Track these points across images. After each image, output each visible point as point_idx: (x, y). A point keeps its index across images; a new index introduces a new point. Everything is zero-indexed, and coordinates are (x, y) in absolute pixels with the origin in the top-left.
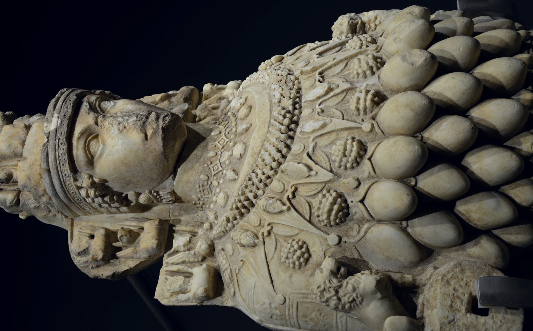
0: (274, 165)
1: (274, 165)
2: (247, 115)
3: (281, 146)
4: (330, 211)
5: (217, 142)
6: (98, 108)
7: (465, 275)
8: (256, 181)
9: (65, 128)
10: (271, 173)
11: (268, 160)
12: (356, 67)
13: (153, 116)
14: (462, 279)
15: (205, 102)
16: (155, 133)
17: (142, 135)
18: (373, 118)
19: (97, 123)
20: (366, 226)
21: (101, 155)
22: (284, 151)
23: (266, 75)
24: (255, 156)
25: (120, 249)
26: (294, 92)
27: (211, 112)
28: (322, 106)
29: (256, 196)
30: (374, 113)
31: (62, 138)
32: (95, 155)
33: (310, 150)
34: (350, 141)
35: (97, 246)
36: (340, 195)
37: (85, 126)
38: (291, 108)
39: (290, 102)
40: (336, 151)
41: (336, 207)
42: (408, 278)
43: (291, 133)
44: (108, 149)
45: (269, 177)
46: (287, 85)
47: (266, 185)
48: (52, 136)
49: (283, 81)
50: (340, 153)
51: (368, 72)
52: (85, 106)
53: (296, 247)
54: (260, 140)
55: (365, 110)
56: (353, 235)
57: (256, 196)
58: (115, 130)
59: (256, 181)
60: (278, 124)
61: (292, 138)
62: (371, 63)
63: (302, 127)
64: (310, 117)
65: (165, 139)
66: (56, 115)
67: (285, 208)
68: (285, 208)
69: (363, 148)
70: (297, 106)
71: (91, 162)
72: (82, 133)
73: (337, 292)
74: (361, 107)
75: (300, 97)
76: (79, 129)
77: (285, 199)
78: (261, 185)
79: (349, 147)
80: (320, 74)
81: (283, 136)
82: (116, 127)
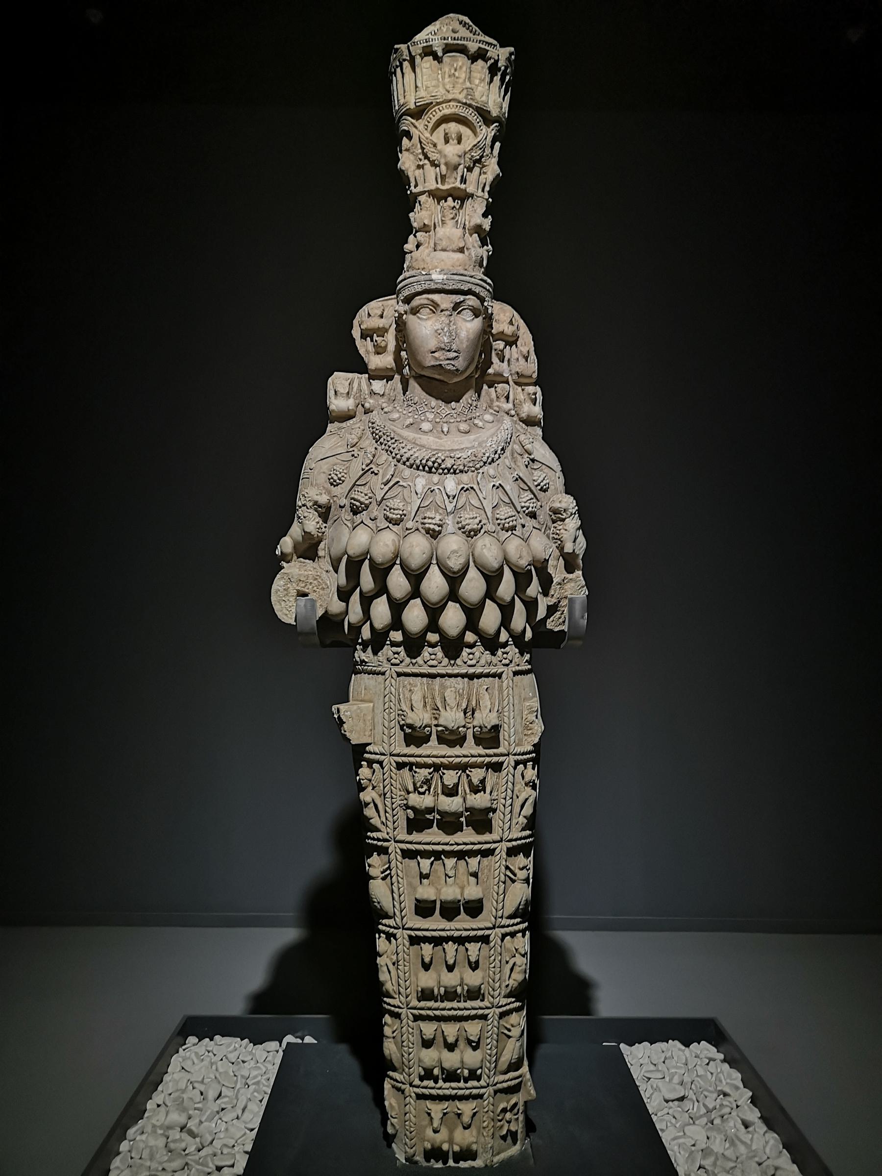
0: (398, 457)
1: (398, 457)
2: (459, 431)
3: (411, 461)
4: (355, 500)
8: (389, 443)
9: (433, 286)
10: (394, 455)
11: (402, 451)
12: (467, 516)
13: (453, 355)
15: (520, 389)
16: (436, 359)
17: (434, 350)
18: (418, 529)
19: (442, 311)
21: (419, 318)
22: (408, 463)
25: (372, 340)
26: (461, 467)
28: (437, 491)
29: (381, 444)
30: (420, 529)
31: (426, 286)
33: (401, 483)
34: (401, 512)
35: (375, 323)
36: (367, 506)
37: (439, 303)
38: (443, 466)
39: (449, 466)
40: (396, 503)
41: (358, 504)
42: (321, 553)
43: (421, 468)
44: (423, 323)
45: (391, 453)
47: (387, 451)
48: (427, 277)
49: (474, 458)
50: (392, 506)
51: (460, 525)
52: (459, 298)
53: (340, 476)
55: (423, 523)
56: (346, 515)
57: (381, 444)
58: (438, 326)
59: (389, 443)
61: (418, 468)
62: (468, 528)
64: (429, 482)
66: (445, 277)
67: (364, 467)
68: (364, 467)
69: (397, 523)
70: (446, 471)
71: (415, 311)
72: (432, 301)
73: (304, 505)
74: (426, 521)
75: (455, 473)
76: (436, 297)
77: (371, 466)
79: (396, 512)
80: (472, 488)
81: (418, 462)
82: (439, 327)
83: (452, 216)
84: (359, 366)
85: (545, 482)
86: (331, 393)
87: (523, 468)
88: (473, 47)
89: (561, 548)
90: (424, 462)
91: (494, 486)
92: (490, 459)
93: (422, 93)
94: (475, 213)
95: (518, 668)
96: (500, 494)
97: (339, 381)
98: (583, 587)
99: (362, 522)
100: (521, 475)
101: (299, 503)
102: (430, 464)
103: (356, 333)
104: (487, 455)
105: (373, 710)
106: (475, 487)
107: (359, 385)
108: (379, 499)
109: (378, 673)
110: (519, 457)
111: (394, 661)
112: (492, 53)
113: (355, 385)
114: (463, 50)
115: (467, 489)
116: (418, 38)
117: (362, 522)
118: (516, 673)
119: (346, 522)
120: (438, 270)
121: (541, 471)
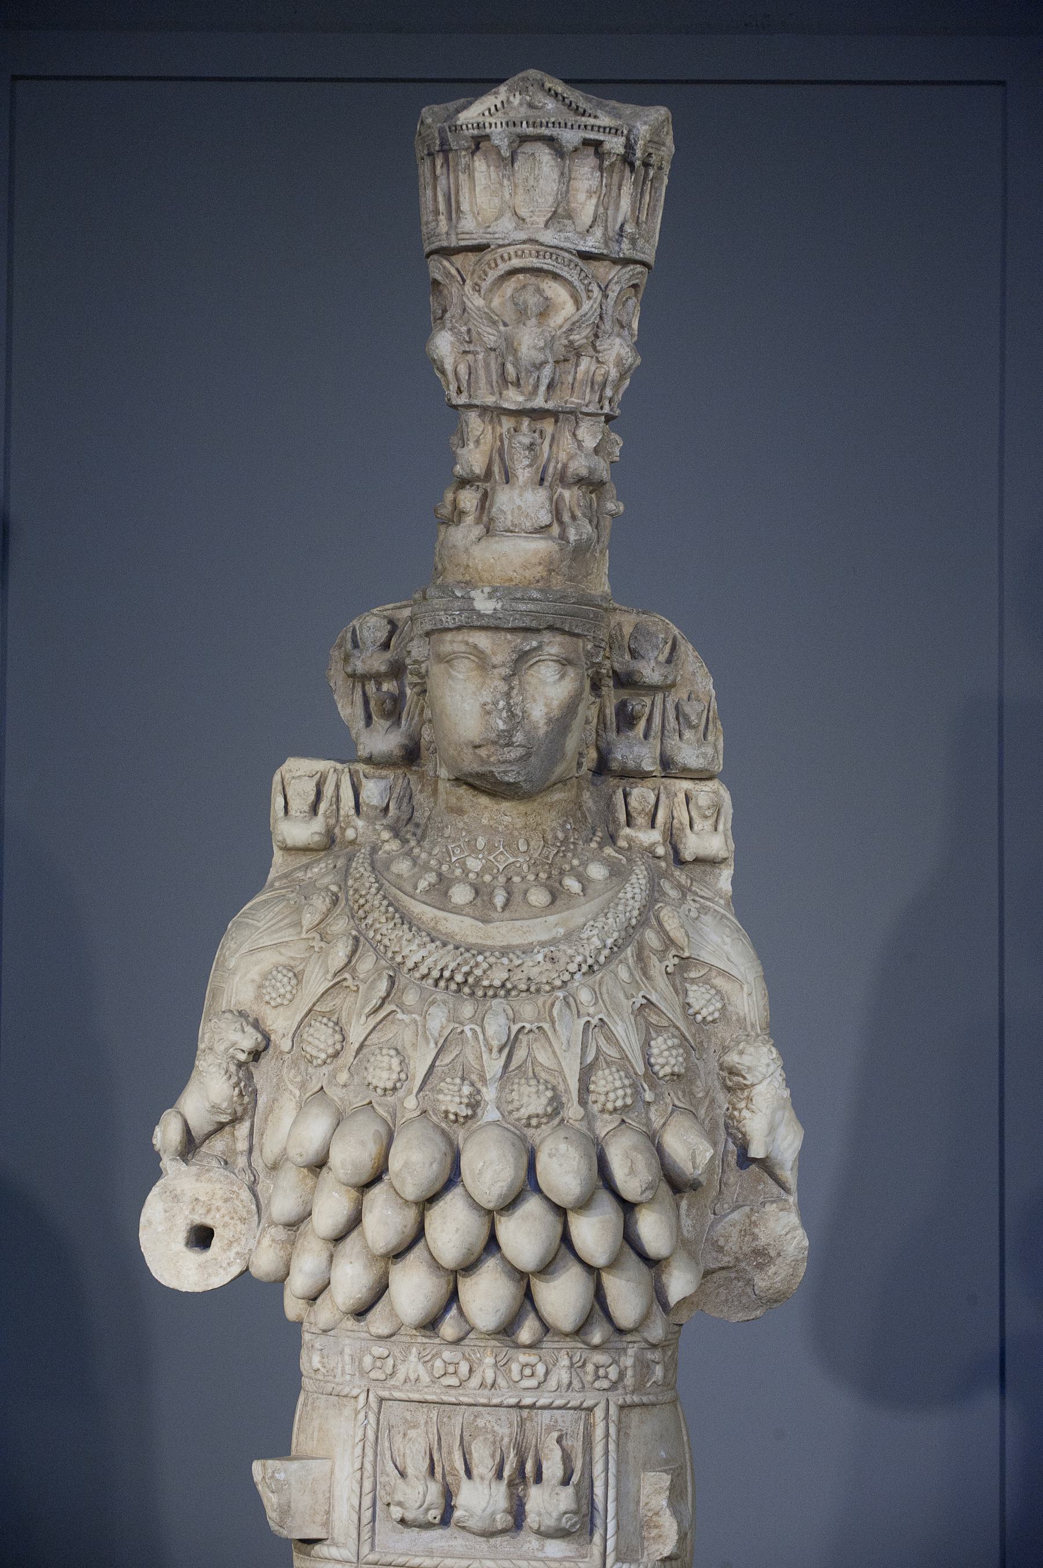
0: (399, 959)
3: (424, 970)
5: (502, 849)
6: (537, 659)
7: (238, 1222)
10: (390, 955)
14: (232, 1218)
16: (483, 762)
17: (477, 742)
20: (297, 1093)
23: (591, 934)
24: (432, 924)
27: (640, 814)
32: (451, 666)
37: (488, 652)
38: (486, 983)
39: (497, 983)
46: (541, 973)
54: (457, 930)
60: (452, 965)
63: (445, 1002)
65: (477, 773)
68: (329, 976)
70: (490, 993)
76: (482, 640)
77: (347, 975)
78: (378, 937)
81: (435, 974)
83: (526, 462)
84: (338, 746)
85: (711, 1009)
86: (278, 802)
87: (662, 982)
88: (570, 138)
89: (743, 1148)
90: (447, 974)
91: (588, 1022)
92: (585, 968)
93: (468, 224)
94: (582, 447)
95: (629, 1399)
96: (602, 1042)
97: (298, 775)
98: (794, 1229)
99: (322, 1088)
100: (654, 998)
101: (201, 1046)
102: (459, 978)
103: (337, 679)
104: (579, 959)
105: (332, 1473)
106: (546, 1026)
107: (337, 787)
108: (357, 1045)
109: (346, 1396)
110: (654, 960)
111: (373, 1375)
112: (615, 145)
113: (329, 790)
114: (550, 141)
115: (531, 1031)
116: (463, 117)
117: (322, 1088)
118: (622, 1408)
119: (291, 1087)
120: (487, 590)
121: (706, 983)
